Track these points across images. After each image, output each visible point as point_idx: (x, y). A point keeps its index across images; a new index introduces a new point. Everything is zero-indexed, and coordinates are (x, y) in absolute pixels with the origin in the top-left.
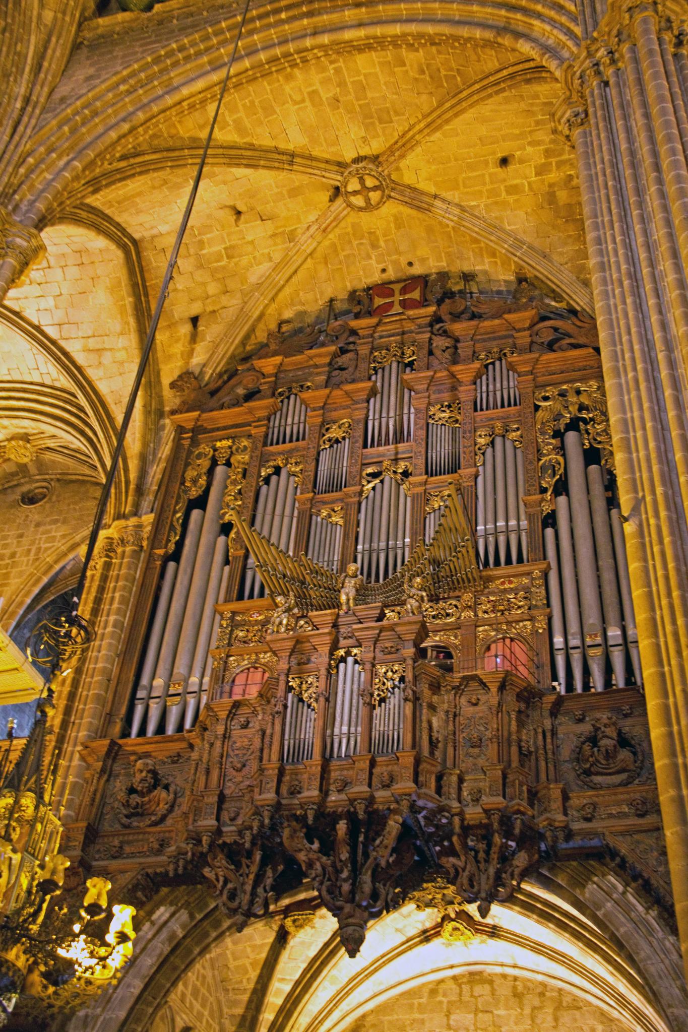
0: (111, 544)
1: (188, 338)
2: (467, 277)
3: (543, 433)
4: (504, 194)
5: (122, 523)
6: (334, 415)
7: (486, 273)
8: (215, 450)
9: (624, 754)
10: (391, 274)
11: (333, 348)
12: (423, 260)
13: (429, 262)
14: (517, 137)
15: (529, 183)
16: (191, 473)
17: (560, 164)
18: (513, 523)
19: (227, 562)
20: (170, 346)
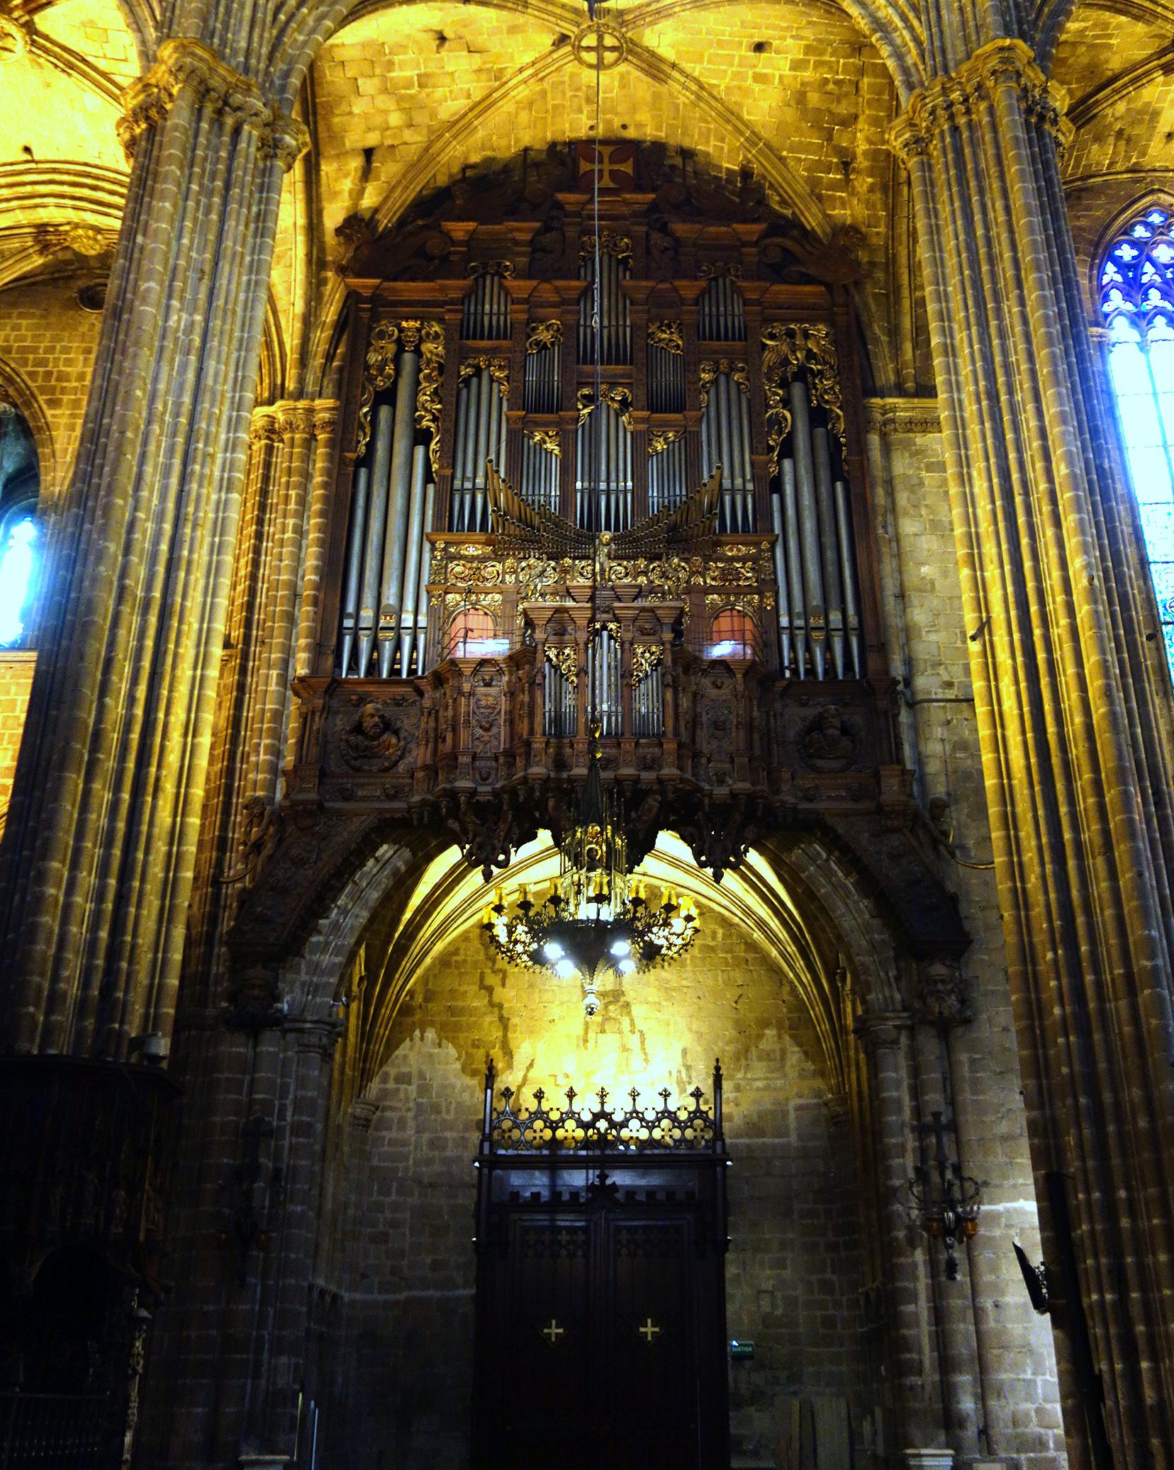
0: (272, 423)
1: (359, 174)
2: (687, 154)
3: (770, 380)
4: (750, 80)
5: (291, 404)
6: (542, 312)
7: (708, 154)
8: (401, 330)
9: (845, 743)
10: (601, 132)
11: (538, 225)
12: (639, 126)
13: (646, 125)
14: (782, 29)
15: (781, 77)
16: (373, 358)
17: (818, 64)
18: (739, 481)
19: (428, 478)
20: (336, 180)
